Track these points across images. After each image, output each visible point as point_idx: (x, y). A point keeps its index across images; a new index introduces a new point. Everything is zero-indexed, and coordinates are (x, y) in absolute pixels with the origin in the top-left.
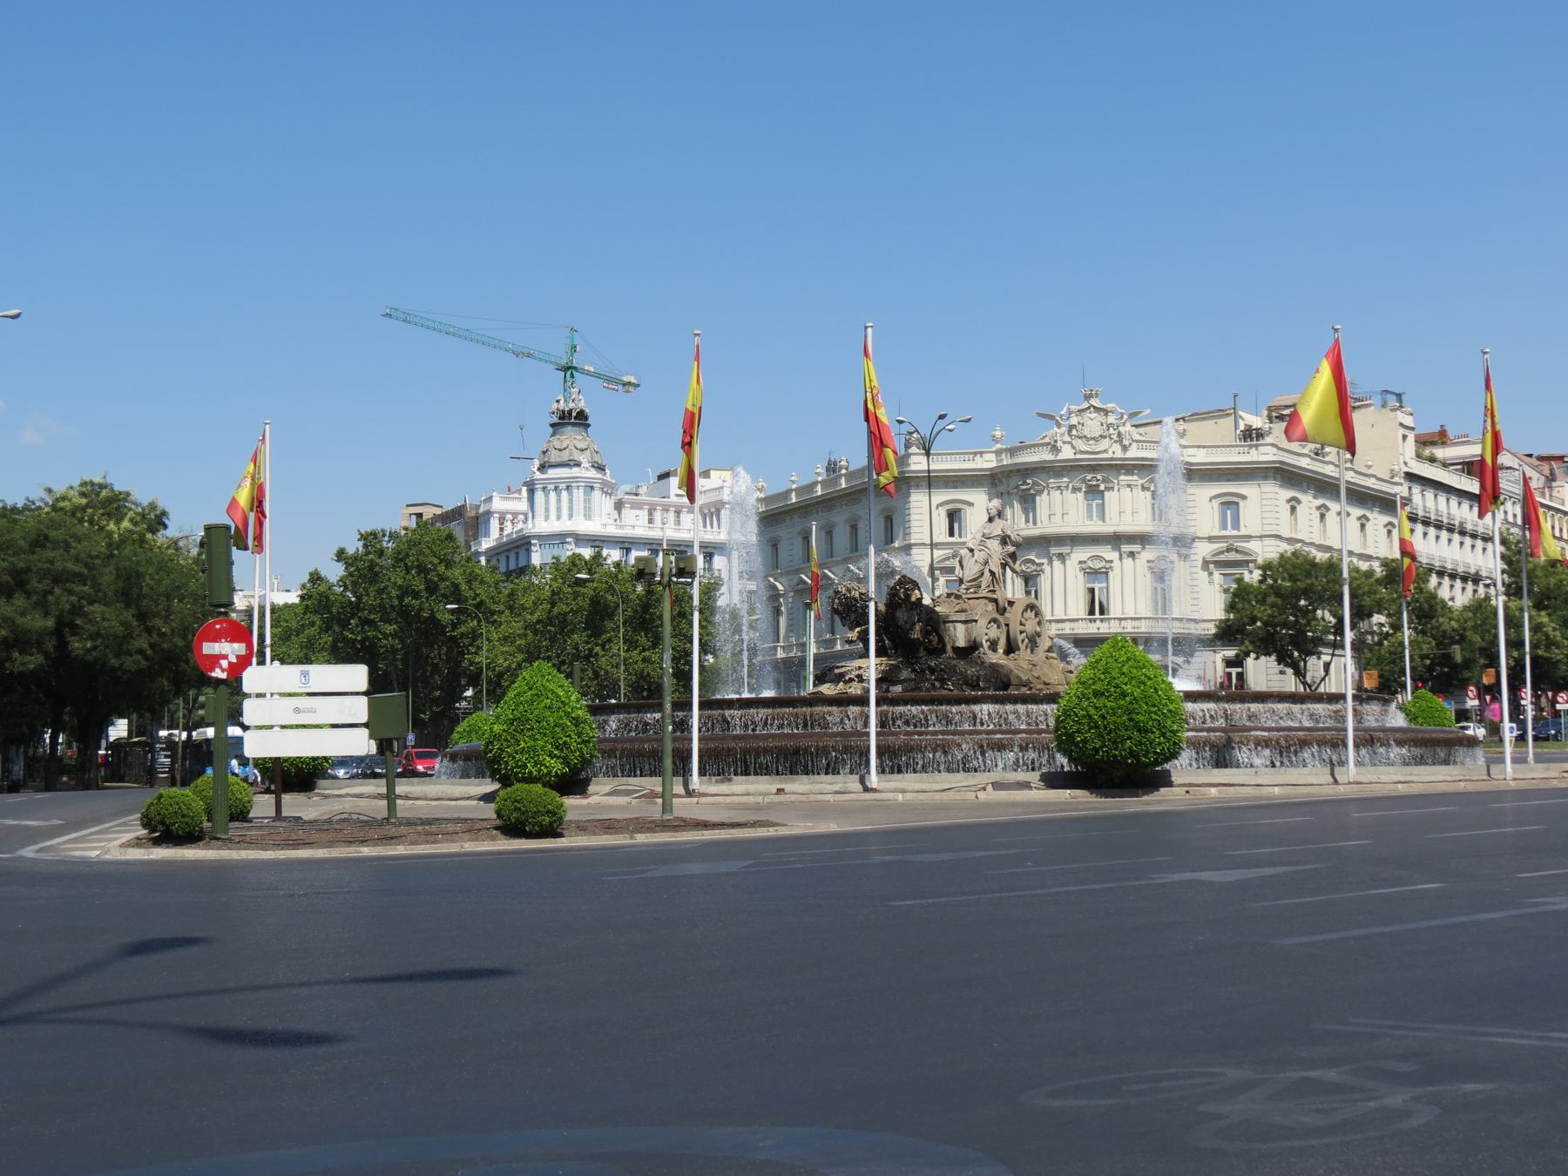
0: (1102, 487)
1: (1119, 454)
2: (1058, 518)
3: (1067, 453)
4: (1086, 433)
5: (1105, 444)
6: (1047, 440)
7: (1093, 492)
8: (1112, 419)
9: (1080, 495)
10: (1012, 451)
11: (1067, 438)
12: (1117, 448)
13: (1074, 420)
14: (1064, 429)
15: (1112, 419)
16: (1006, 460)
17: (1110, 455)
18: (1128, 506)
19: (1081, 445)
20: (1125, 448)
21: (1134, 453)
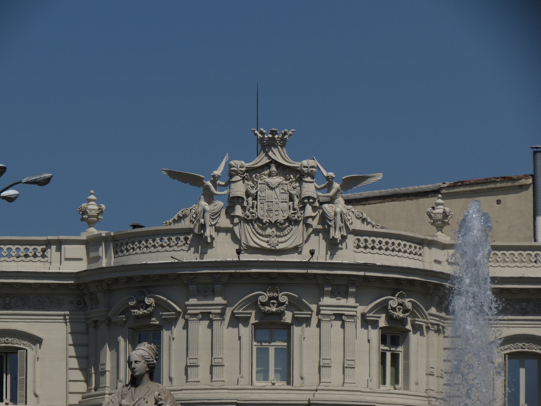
0: (288, 317)
1: (322, 256)
2: (202, 373)
3: (223, 250)
4: (261, 213)
5: (295, 236)
6: (186, 224)
7: (271, 327)
8: (310, 189)
9: (246, 332)
10: (118, 243)
11: (224, 222)
12: (318, 244)
13: (239, 188)
14: (219, 204)
15: (310, 189)
16: (107, 260)
17: (304, 257)
18: (335, 357)
19: (250, 236)
20: (333, 246)
21: (348, 254)
